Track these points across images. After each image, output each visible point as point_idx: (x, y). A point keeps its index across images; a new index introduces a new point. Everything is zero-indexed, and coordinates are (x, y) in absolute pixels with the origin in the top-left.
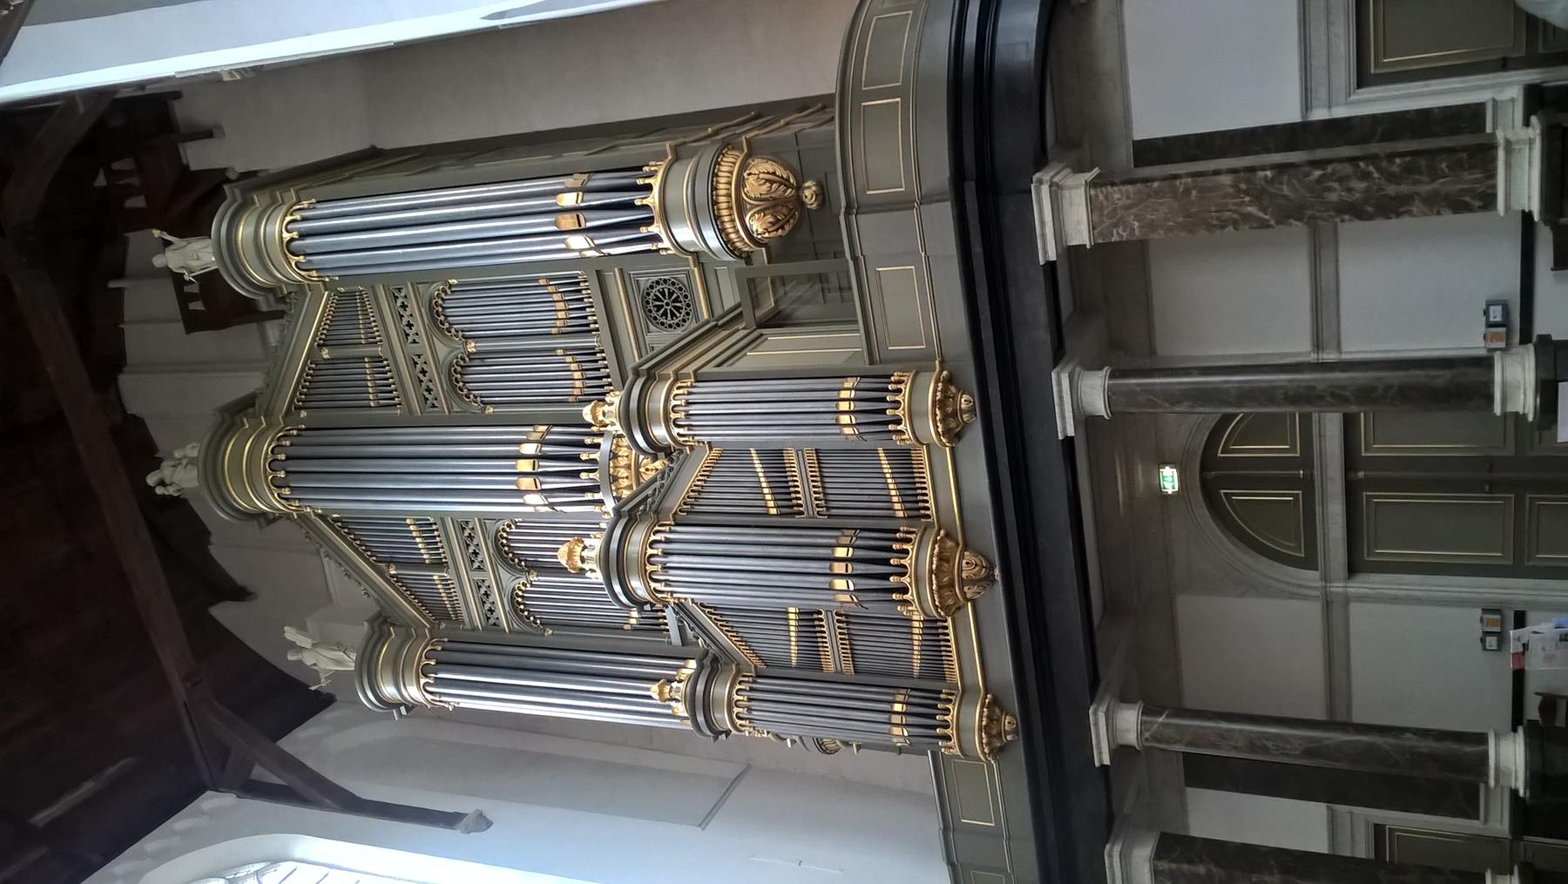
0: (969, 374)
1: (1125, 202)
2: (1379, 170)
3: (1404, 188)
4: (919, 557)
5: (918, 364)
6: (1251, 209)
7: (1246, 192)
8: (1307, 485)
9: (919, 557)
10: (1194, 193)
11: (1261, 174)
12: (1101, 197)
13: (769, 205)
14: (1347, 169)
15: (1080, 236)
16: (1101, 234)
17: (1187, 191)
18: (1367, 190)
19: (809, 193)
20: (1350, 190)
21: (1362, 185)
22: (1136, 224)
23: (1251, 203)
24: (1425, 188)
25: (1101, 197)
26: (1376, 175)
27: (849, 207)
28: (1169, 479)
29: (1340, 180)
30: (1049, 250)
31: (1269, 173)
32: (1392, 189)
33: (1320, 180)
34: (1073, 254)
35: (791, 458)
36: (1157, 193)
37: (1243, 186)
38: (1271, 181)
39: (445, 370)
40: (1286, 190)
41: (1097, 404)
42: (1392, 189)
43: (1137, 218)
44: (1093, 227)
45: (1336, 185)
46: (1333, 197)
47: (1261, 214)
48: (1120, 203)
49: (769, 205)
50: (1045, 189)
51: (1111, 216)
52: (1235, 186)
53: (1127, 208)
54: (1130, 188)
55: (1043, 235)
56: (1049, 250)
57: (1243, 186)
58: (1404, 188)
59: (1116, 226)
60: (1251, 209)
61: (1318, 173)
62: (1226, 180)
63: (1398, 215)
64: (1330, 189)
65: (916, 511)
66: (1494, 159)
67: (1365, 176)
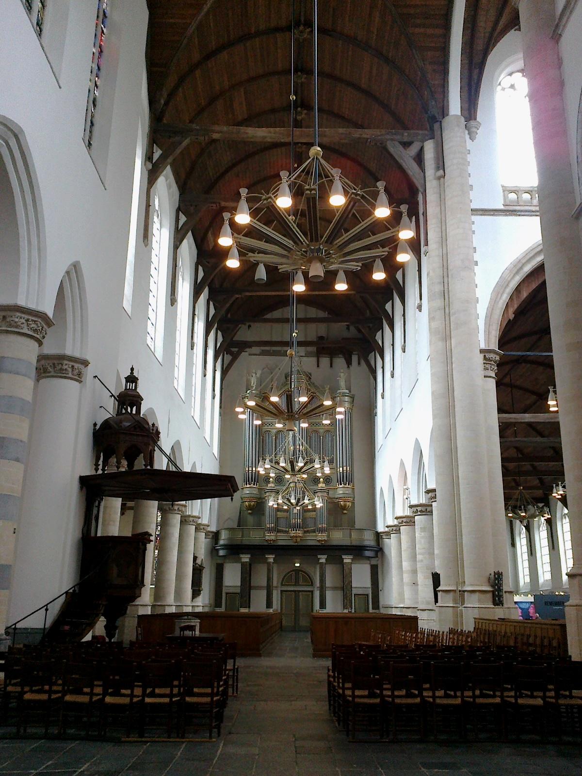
0: (328, 544)
4: (300, 533)
5: (328, 536)
8: (295, 585)
9: (300, 533)
13: (345, 505)
15: (345, 561)
19: (345, 512)
28: (297, 565)
30: (344, 557)
32: (348, 599)
34: (343, 559)
35: (314, 513)
39: (317, 430)
41: (321, 561)
42: (348, 599)
46: (348, 592)
49: (345, 505)
56: (344, 557)
65: (305, 532)
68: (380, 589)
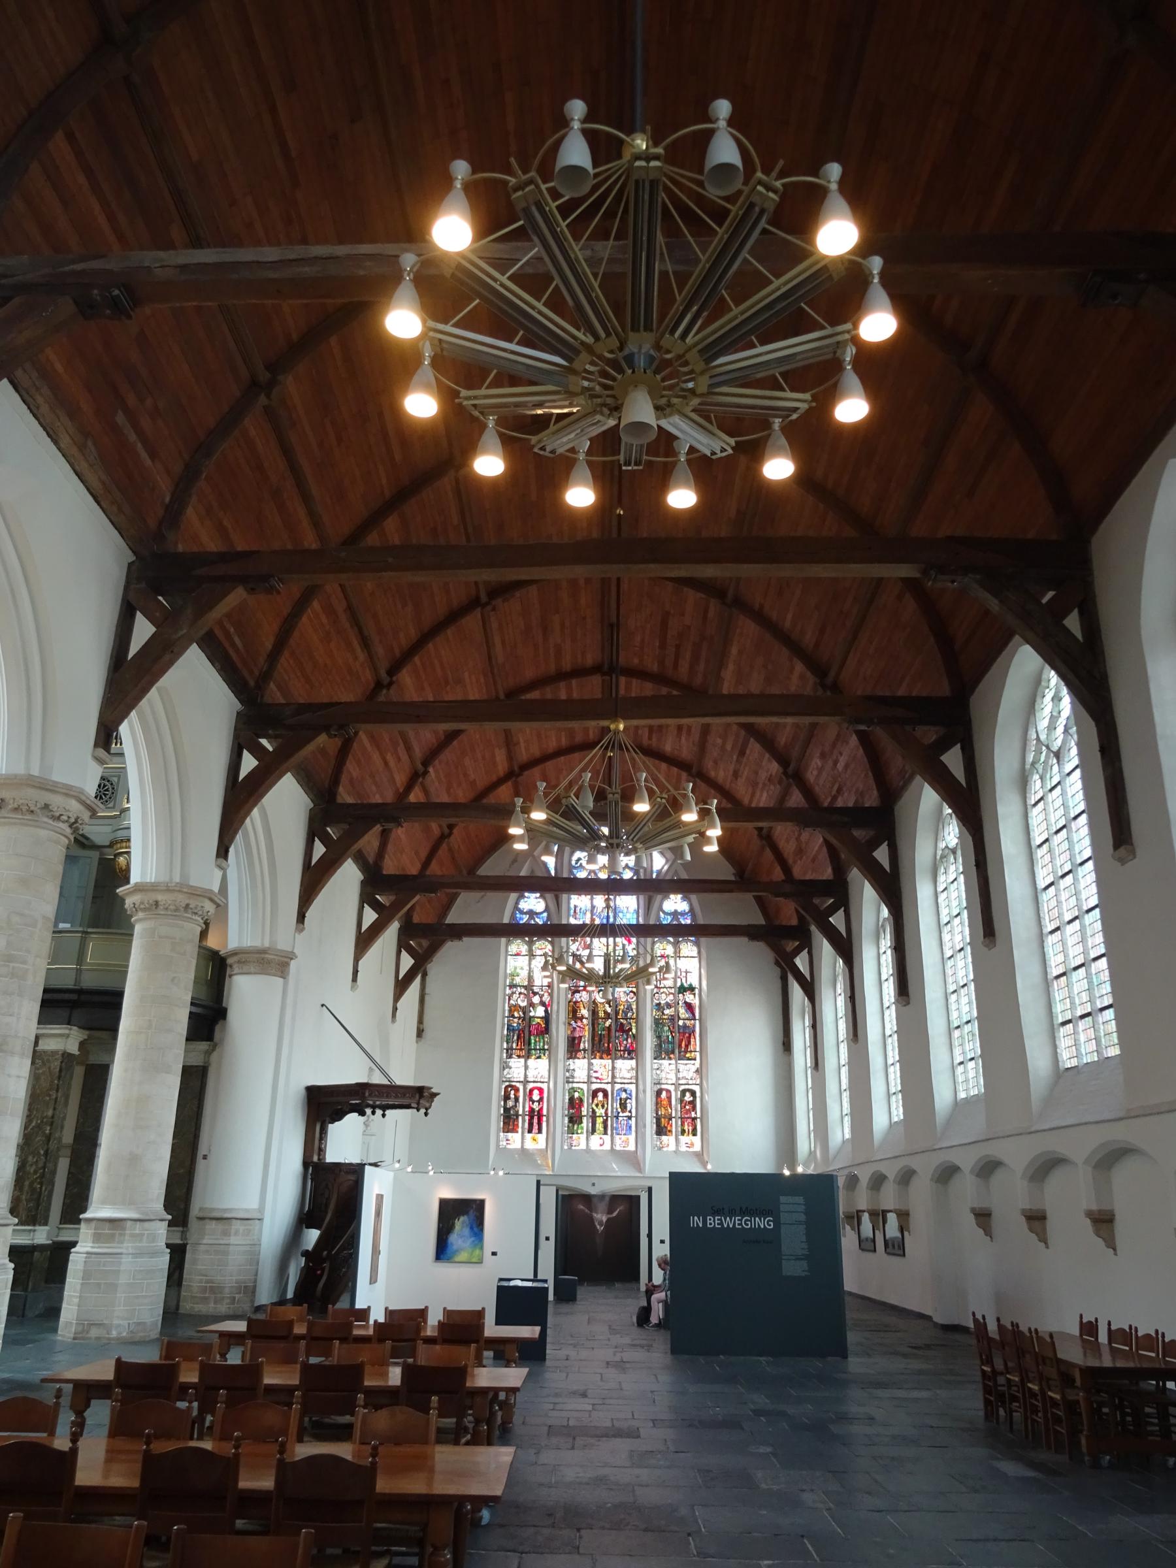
1: (52, 1068)
2: (37, 1178)
3: (26, 1188)
6: (33, 1124)
7: (42, 1122)
10: (48, 1098)
11: (48, 1128)
12: (57, 1057)
14: (41, 1164)
16: (41, 1054)
17: (50, 1096)
18: (29, 1173)
20: (31, 1165)
21: (32, 1171)
22: (41, 1071)
23: (37, 1123)
24: (24, 1197)
25: (57, 1057)
26: (35, 1177)
27: (87, 933)
29: (37, 1161)
31: (47, 1132)
32: (27, 1183)
33: (39, 1153)
36: (52, 1082)
37: (45, 1120)
38: (44, 1132)
40: (39, 1138)
42: (27, 1183)
43: (43, 1073)
44: (45, 1052)
45: (35, 1160)
46: (30, 1158)
47: (31, 1127)
48: (52, 1065)
50: (67, 1032)
51: (48, 1061)
52: (46, 1117)
53: (49, 1068)
54: (58, 1070)
55: (46, 1028)
57: (45, 1120)
58: (26, 1188)
59: (43, 1062)
60: (33, 1124)
61: (42, 1152)
62: (50, 1113)
63: (15, 1186)
64: (34, 1157)
66: (29, 1225)
67: (35, 1172)
68: (202, 1150)
